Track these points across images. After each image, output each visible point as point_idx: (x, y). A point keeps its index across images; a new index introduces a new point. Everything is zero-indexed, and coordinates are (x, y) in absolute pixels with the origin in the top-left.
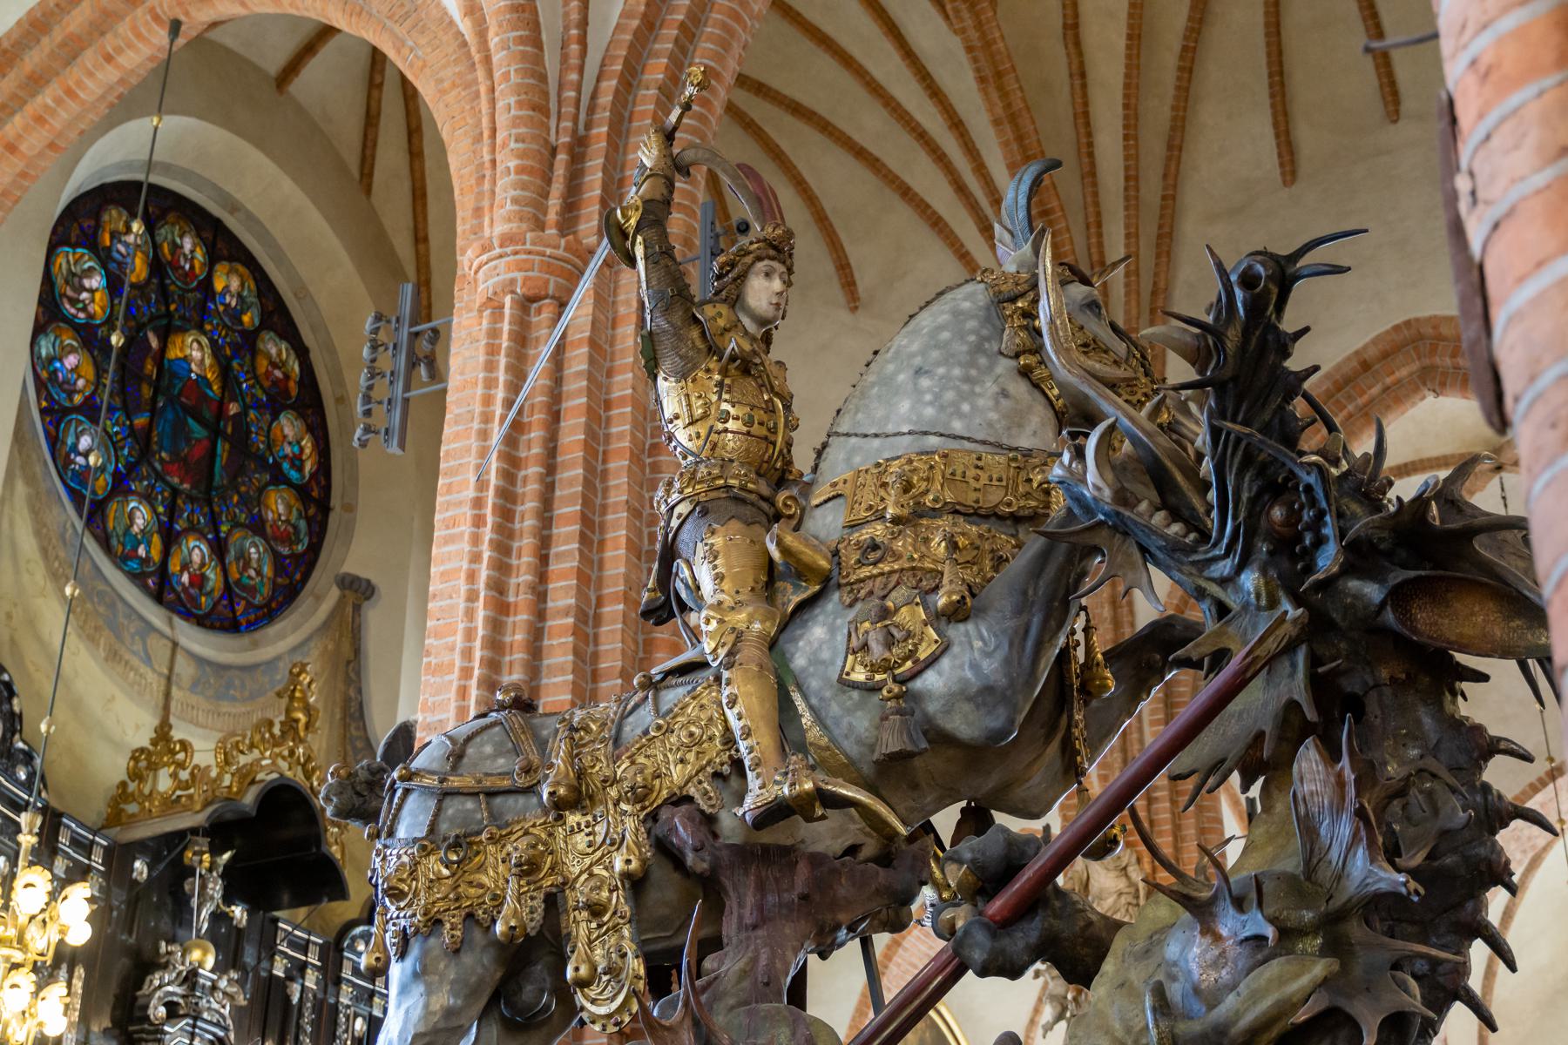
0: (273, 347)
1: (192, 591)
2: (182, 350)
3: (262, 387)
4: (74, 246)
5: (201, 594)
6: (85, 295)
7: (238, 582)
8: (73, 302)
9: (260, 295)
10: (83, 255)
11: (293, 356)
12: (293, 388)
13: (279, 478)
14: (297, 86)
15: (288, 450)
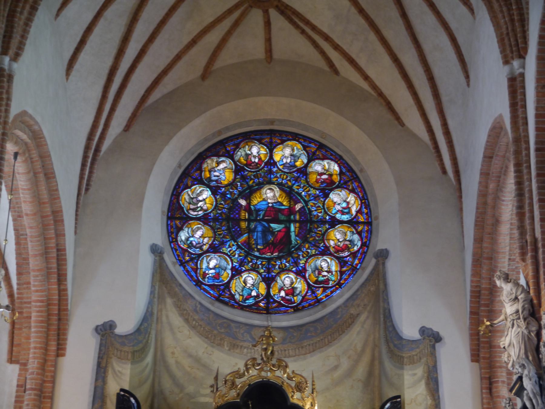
0: (317, 167)
1: (288, 297)
2: (260, 197)
3: (314, 188)
4: (190, 188)
5: (294, 296)
6: (200, 204)
7: (317, 282)
8: (194, 210)
9: (305, 148)
10: (195, 188)
11: (333, 163)
12: (336, 178)
13: (334, 222)
14: (276, 55)
15: (338, 208)
